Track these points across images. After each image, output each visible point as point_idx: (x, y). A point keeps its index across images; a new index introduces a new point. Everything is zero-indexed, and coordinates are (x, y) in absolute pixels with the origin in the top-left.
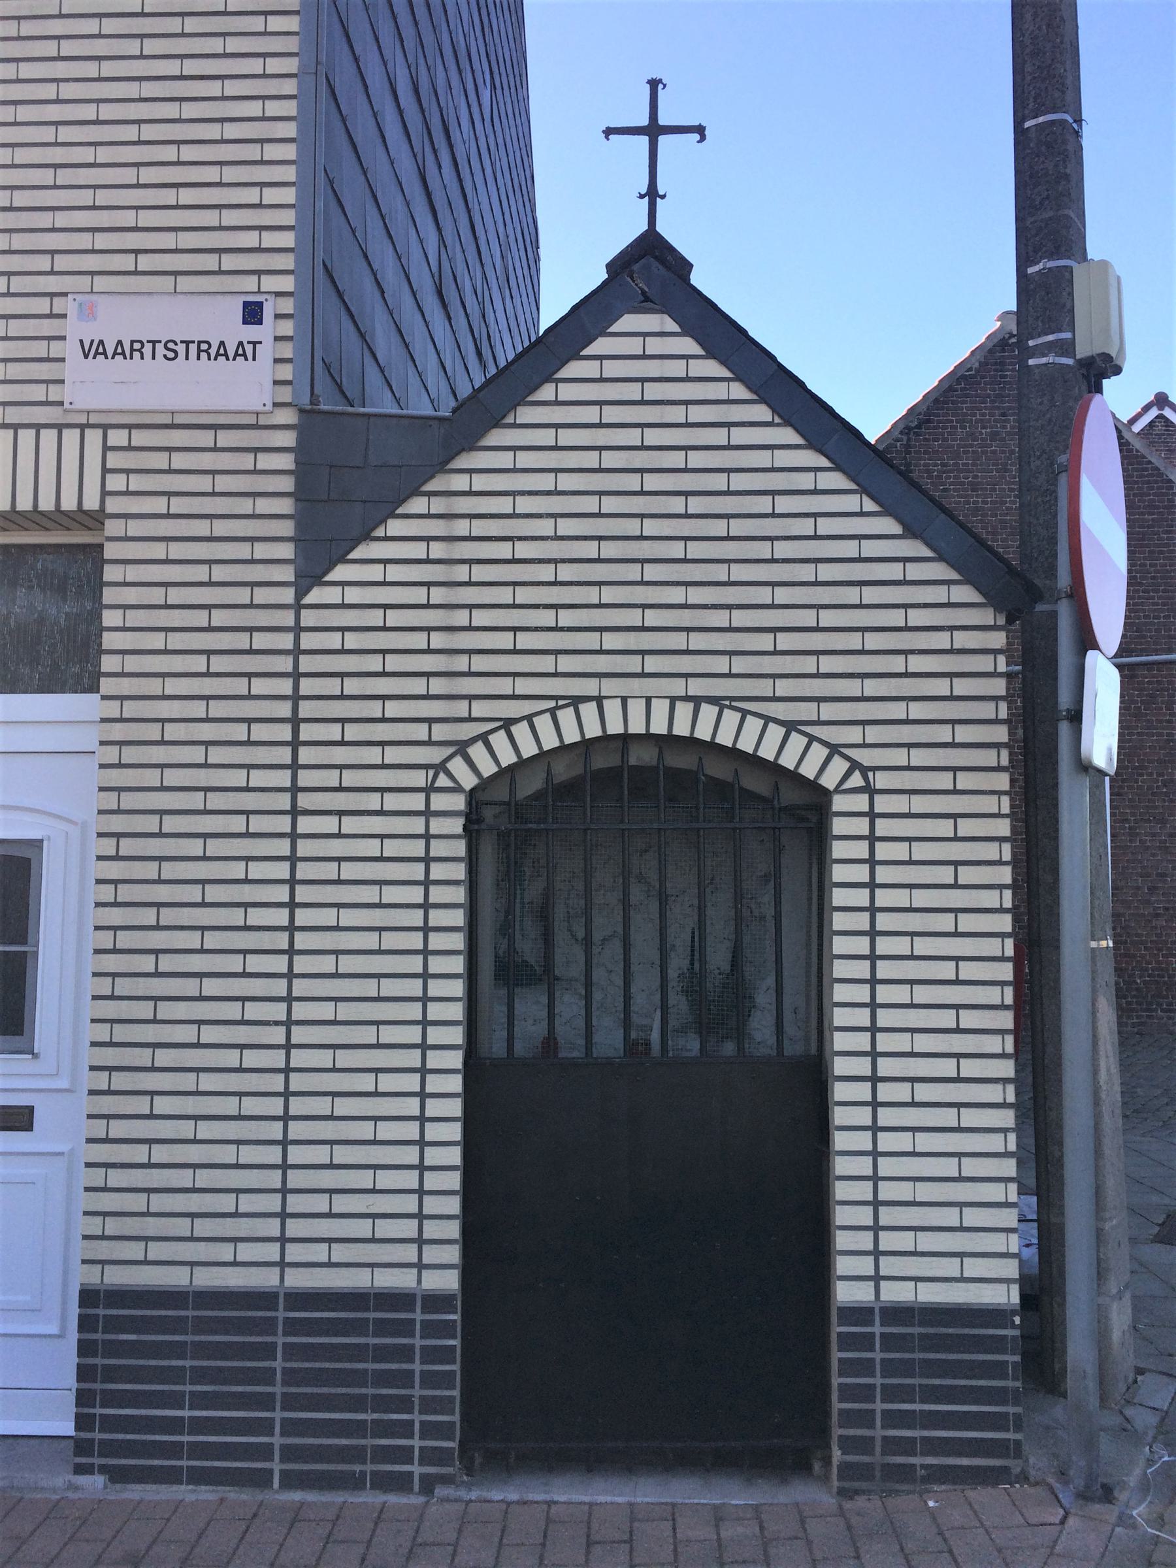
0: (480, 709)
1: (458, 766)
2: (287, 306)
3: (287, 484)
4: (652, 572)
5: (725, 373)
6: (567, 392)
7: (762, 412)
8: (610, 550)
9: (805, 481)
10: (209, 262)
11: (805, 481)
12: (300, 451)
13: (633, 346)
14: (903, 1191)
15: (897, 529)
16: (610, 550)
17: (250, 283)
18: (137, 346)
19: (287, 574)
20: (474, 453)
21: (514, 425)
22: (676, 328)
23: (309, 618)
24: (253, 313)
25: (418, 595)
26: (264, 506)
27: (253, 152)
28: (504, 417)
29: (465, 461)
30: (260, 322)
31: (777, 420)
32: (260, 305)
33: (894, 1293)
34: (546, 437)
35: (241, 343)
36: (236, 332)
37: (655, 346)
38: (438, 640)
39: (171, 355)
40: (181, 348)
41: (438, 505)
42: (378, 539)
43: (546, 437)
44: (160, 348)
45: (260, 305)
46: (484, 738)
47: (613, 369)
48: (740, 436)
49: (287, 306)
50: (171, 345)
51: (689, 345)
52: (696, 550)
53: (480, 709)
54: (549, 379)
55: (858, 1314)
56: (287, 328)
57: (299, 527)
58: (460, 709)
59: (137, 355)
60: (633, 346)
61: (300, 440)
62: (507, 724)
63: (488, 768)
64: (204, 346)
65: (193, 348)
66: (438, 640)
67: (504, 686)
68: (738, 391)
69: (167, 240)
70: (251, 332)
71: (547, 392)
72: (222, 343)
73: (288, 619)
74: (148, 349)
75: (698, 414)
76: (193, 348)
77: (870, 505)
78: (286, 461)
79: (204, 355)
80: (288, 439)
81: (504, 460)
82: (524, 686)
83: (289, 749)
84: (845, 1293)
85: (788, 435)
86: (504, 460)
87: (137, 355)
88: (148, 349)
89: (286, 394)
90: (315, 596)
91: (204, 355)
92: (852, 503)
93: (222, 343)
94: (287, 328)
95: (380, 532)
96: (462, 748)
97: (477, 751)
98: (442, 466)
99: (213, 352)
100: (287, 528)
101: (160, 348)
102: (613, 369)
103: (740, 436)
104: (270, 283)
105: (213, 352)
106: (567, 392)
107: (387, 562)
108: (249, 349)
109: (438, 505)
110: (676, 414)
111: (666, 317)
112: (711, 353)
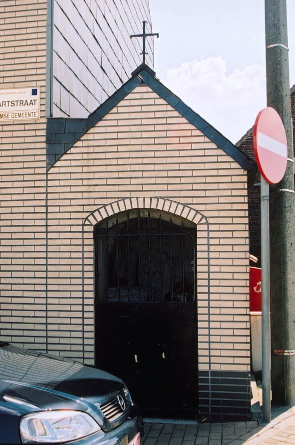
0: (97, 202)
1: (91, 218)
2: (44, 89)
3: (44, 139)
4: (145, 161)
5: (165, 103)
6: (121, 110)
7: (176, 114)
8: (133, 155)
9: (188, 133)
10: (23, 79)
11: (188, 133)
12: (48, 129)
13: (139, 96)
14: (217, 325)
15: (215, 146)
16: (133, 155)
17: (34, 84)
18: (4, 103)
19: (44, 164)
20: (95, 128)
21: (106, 120)
22: (151, 90)
23: (50, 177)
24: (34, 92)
25: (79, 169)
26: (38, 145)
27: (34, 48)
28: (103, 118)
29: (92, 130)
30: (36, 94)
31: (180, 116)
32: (36, 90)
33: (215, 368)
34: (115, 123)
35: (31, 101)
36: (29, 97)
37: (145, 96)
38: (85, 182)
39: (13, 105)
40: (15, 103)
41: (85, 143)
42: (68, 154)
43: (115, 123)
44: (10, 103)
45: (36, 90)
46: (98, 210)
47: (133, 103)
48: (169, 121)
49: (44, 89)
50: (13, 102)
51: (155, 95)
52: (157, 154)
53: (97, 202)
54: (115, 106)
55: (205, 373)
56: (44, 95)
57: (47, 151)
58: (91, 202)
59: (4, 105)
60: (139, 96)
61: (47, 127)
62: (104, 206)
63: (99, 219)
64: (22, 102)
65: (19, 102)
66: (85, 182)
67: (103, 195)
68: (169, 108)
69: (12, 73)
70: (35, 97)
71: (114, 110)
72: (26, 101)
73: (44, 177)
74: (7, 104)
75: (158, 115)
76: (19, 102)
77: (207, 140)
78: (44, 133)
79: (21, 104)
80: (44, 126)
81: (103, 130)
82: (109, 195)
83: (45, 208)
84: (201, 367)
85: (184, 120)
86: (103, 130)
87: (4, 105)
88: (7, 104)
89: (43, 114)
90: (52, 170)
91: (21, 104)
92: (202, 139)
93: (26, 101)
94: (44, 95)
95: (69, 152)
96: (92, 213)
97: (96, 214)
98: (85, 132)
99: (24, 103)
100: (44, 152)
101: (10, 103)
102: (133, 103)
103: (169, 121)
104: (39, 83)
105: (24, 103)
106: (121, 110)
107: (72, 159)
108: (33, 102)
109: (85, 143)
110: (151, 115)
111: (148, 87)
112: (161, 97)
